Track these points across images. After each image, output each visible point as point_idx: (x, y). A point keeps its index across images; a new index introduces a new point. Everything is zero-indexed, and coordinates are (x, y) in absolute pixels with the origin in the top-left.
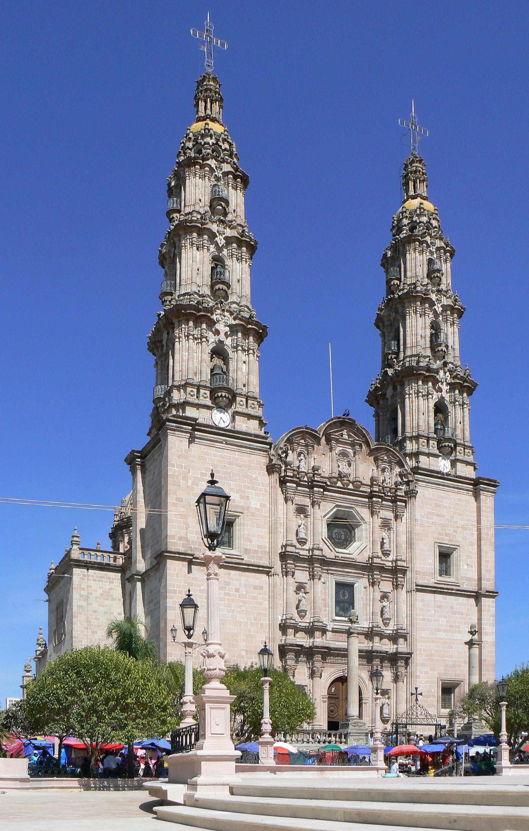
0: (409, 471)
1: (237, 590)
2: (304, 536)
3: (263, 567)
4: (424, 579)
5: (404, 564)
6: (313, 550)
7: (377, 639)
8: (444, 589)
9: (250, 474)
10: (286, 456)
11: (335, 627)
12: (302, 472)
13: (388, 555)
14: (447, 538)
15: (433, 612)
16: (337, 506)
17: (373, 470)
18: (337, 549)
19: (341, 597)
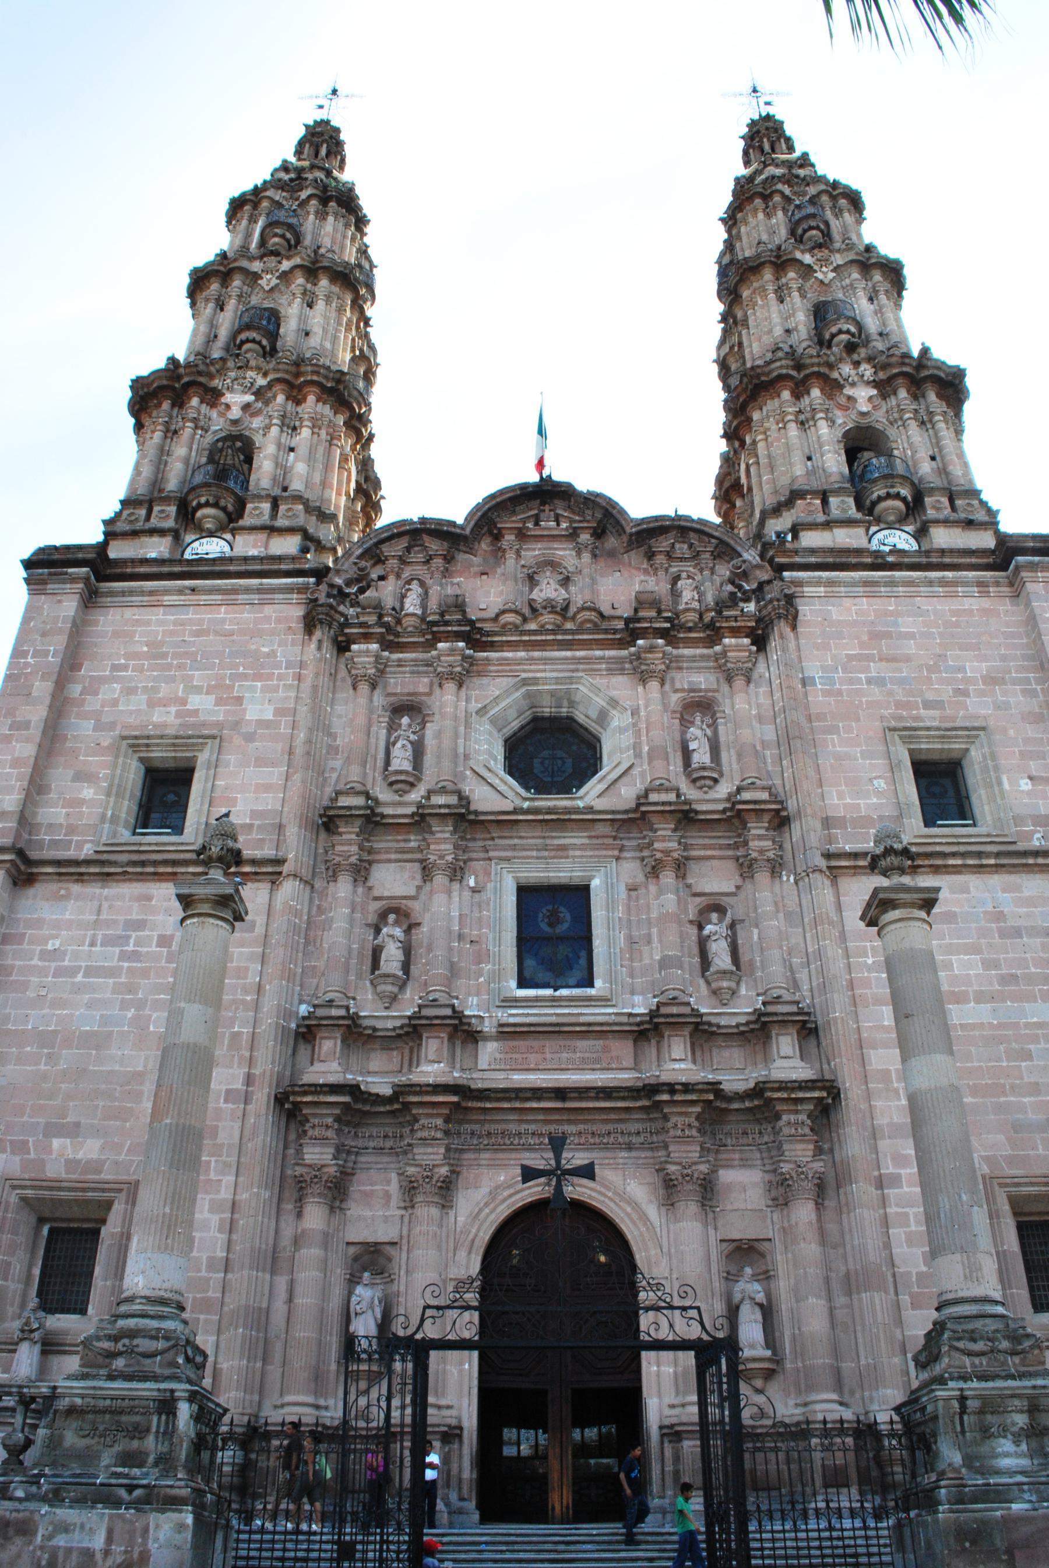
2: (407, 766)
7: (678, 1047)
12: (407, 615)
13: (709, 782)
14: (936, 713)
16: (525, 682)
19: (544, 926)
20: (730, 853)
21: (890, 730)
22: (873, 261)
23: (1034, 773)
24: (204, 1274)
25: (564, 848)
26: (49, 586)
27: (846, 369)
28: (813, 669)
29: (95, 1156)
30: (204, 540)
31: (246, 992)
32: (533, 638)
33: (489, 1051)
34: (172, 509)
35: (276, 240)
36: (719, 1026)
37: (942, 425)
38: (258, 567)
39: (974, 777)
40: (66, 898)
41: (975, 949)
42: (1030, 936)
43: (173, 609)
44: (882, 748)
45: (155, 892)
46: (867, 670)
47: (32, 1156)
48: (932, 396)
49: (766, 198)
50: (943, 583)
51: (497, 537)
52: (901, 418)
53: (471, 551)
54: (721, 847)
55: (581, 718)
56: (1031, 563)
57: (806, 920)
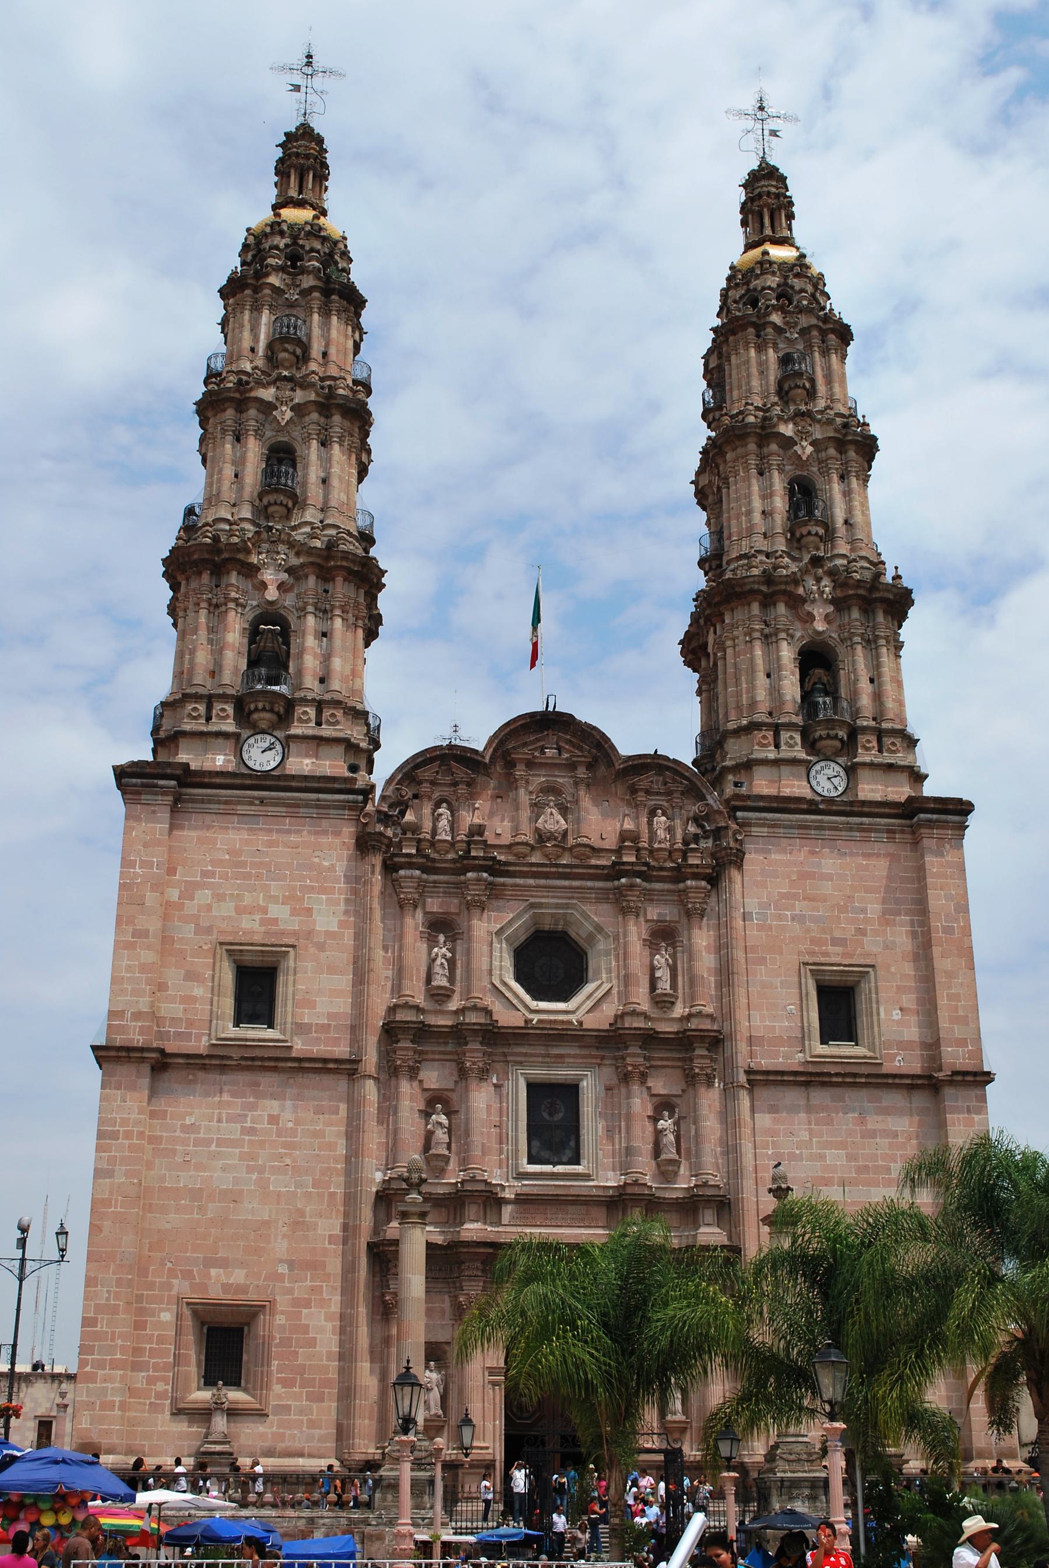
1: (273, 1119)
3: (336, 1061)
4: (776, 1055)
5: (706, 1025)
6: (462, 1011)
8: (829, 1074)
9: (316, 860)
10: (403, 813)
11: (526, 1190)
12: (440, 841)
13: (669, 1005)
14: (839, 949)
15: (805, 1136)
16: (532, 906)
18: (534, 1004)
19: (546, 1115)
20: (679, 1064)
21: (804, 964)
22: (850, 438)
23: (905, 1005)
24: (325, 1362)
25: (561, 1056)
26: (143, 797)
27: (810, 583)
28: (752, 905)
29: (242, 1282)
30: (258, 737)
31: (336, 1161)
32: (540, 869)
33: (507, 1211)
34: (230, 709)
36: (664, 1199)
37: (884, 650)
38: (316, 785)
39: (862, 1005)
40: (194, 1082)
41: (842, 1145)
42: (882, 1137)
43: (246, 818)
44: (796, 979)
45: (262, 1080)
46: (792, 907)
47: (198, 1280)
48: (880, 618)
49: (759, 328)
50: (860, 828)
51: (510, 764)
52: (851, 640)
53: (488, 775)
54: (674, 1059)
55: (573, 935)
56: (930, 821)
57: (729, 1120)
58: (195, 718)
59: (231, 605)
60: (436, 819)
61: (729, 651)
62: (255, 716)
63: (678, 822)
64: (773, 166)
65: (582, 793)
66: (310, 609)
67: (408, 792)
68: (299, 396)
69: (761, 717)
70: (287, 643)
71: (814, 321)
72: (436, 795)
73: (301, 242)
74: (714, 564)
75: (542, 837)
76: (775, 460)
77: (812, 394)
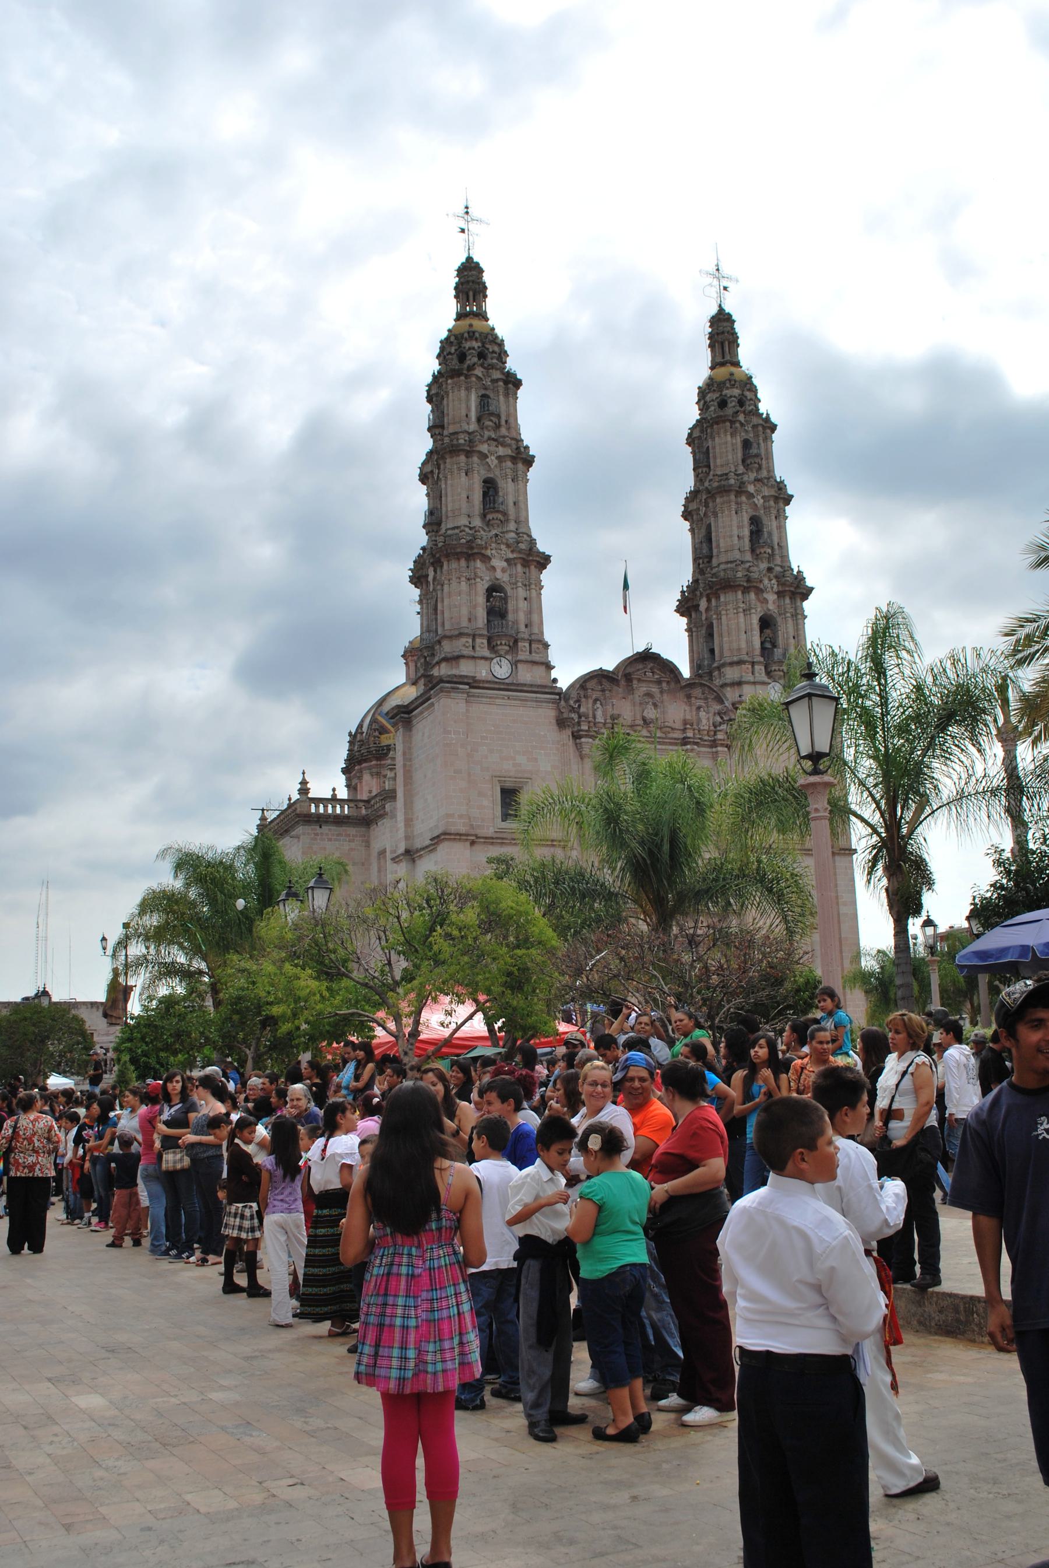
0: (730, 707)
10: (579, 706)
17: (685, 711)
26: (452, 694)
27: (766, 581)
34: (485, 641)
35: (490, 423)
38: (536, 690)
49: (732, 422)
53: (618, 685)
58: (467, 647)
59: (478, 580)
60: (594, 710)
61: (724, 617)
62: (500, 647)
63: (711, 715)
64: (729, 314)
65: (665, 697)
66: (520, 584)
67: (582, 693)
68: (501, 451)
69: (746, 658)
70: (506, 603)
71: (761, 422)
72: (594, 697)
73: (487, 346)
74: (706, 560)
75: (646, 722)
76: (744, 506)
77: (760, 468)
